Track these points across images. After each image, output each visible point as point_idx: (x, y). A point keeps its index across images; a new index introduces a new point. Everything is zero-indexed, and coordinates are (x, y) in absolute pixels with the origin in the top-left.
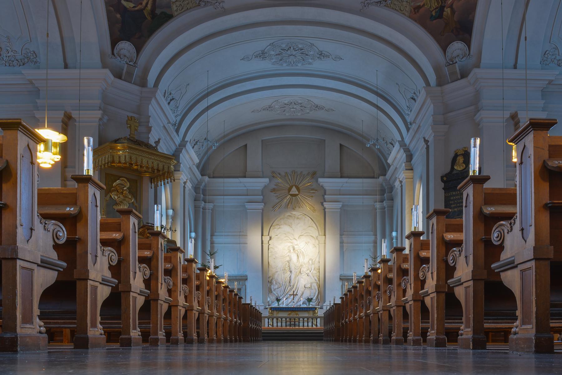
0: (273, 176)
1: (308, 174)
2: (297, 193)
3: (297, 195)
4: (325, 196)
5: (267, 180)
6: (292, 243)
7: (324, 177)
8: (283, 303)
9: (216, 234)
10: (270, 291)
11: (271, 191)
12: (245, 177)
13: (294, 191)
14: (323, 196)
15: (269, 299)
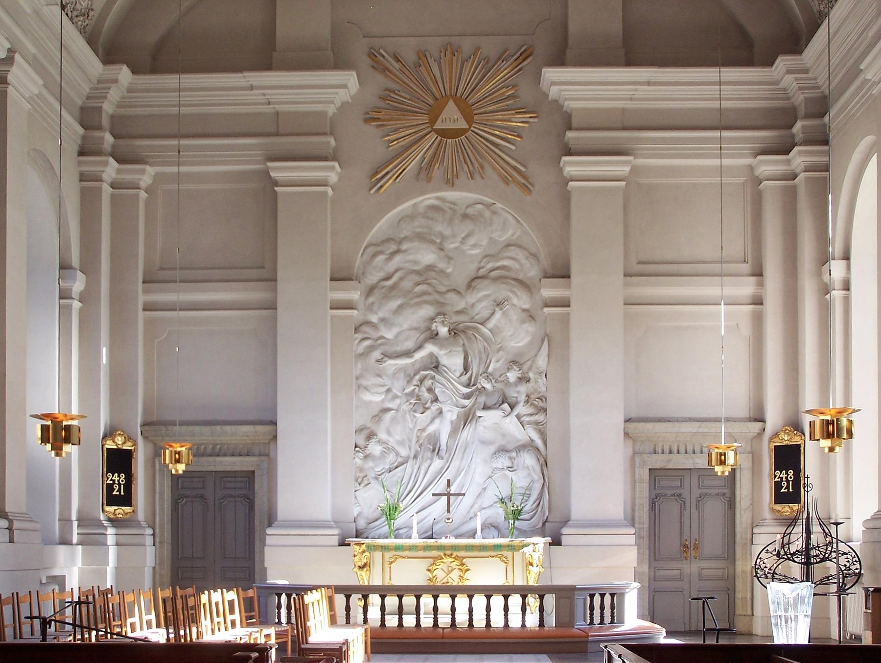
1: (502, 57)
3: (462, 132)
4: (570, 134)
5: (350, 79)
12: (268, 66)
13: (451, 117)
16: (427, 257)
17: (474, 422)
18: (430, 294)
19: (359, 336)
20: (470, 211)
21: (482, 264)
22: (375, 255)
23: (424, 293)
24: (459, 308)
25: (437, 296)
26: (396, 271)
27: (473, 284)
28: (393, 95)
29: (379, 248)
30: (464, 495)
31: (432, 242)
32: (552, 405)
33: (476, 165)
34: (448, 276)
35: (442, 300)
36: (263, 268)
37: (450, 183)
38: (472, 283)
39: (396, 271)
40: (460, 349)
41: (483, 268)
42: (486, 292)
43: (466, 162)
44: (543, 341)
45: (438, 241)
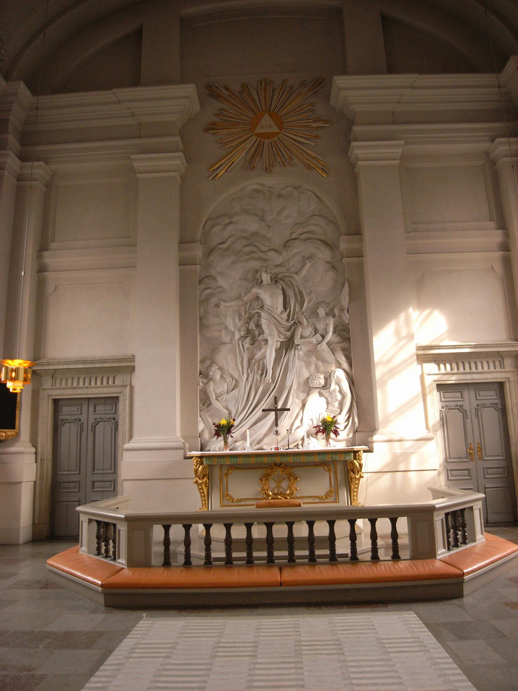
0: (211, 92)
2: (275, 129)
6: (265, 260)
7: (345, 73)
8: (244, 437)
9: (53, 245)
10: (206, 401)
11: (206, 130)
13: (267, 124)
14: (350, 129)
15: (201, 426)
16: (252, 225)
17: (294, 348)
18: (255, 253)
19: (202, 287)
20: (283, 192)
21: (294, 230)
22: (213, 226)
23: (252, 252)
24: (278, 263)
25: (261, 255)
26: (229, 237)
27: (288, 244)
28: (224, 112)
29: (217, 221)
30: (289, 410)
31: (256, 215)
32: (354, 334)
33: (286, 157)
34: (268, 239)
35: (265, 257)
36: (129, 237)
37: (268, 170)
38: (286, 244)
39: (229, 237)
40: (280, 292)
41: (294, 232)
42: (298, 248)
43: (279, 155)
44: (343, 285)
45: (261, 214)
